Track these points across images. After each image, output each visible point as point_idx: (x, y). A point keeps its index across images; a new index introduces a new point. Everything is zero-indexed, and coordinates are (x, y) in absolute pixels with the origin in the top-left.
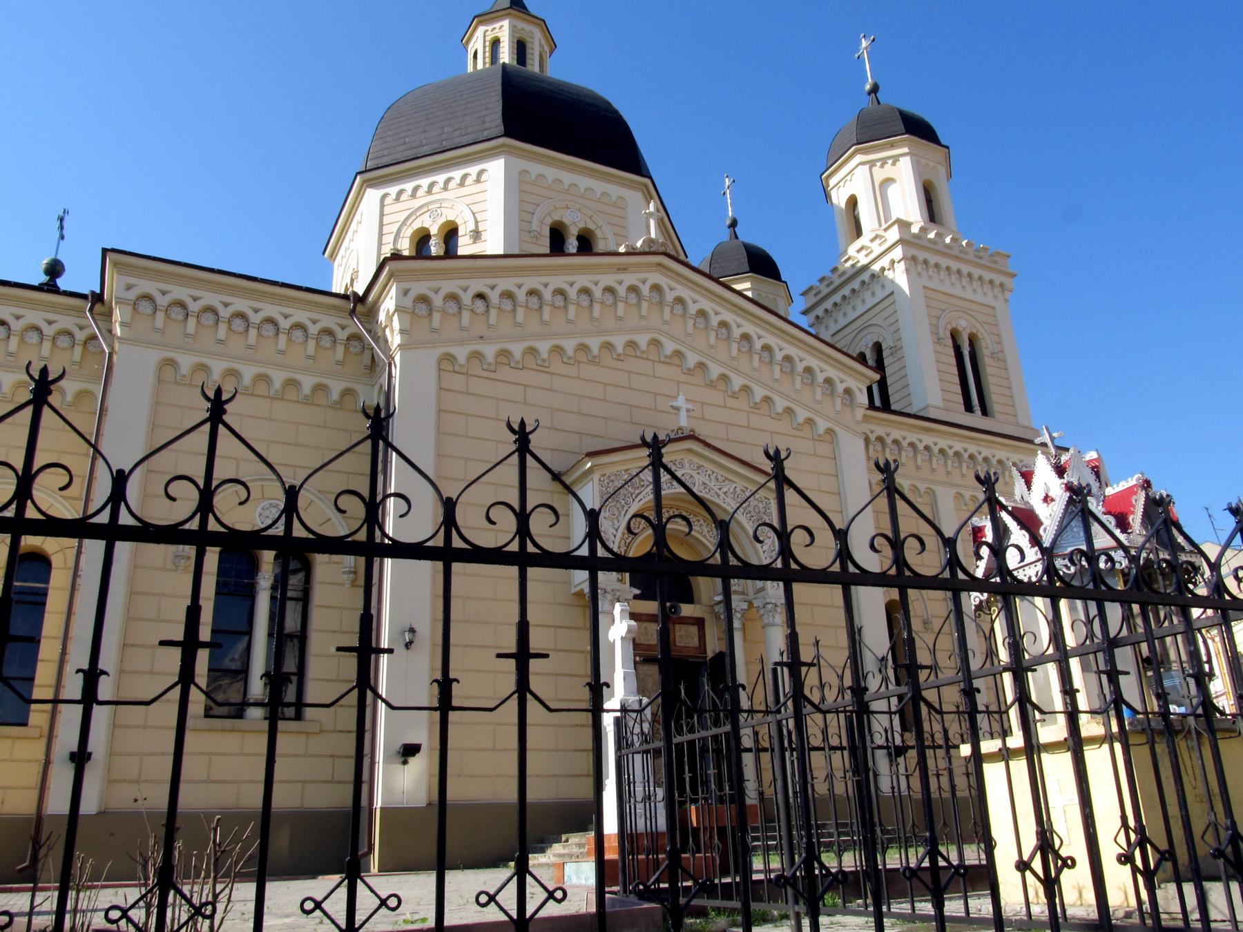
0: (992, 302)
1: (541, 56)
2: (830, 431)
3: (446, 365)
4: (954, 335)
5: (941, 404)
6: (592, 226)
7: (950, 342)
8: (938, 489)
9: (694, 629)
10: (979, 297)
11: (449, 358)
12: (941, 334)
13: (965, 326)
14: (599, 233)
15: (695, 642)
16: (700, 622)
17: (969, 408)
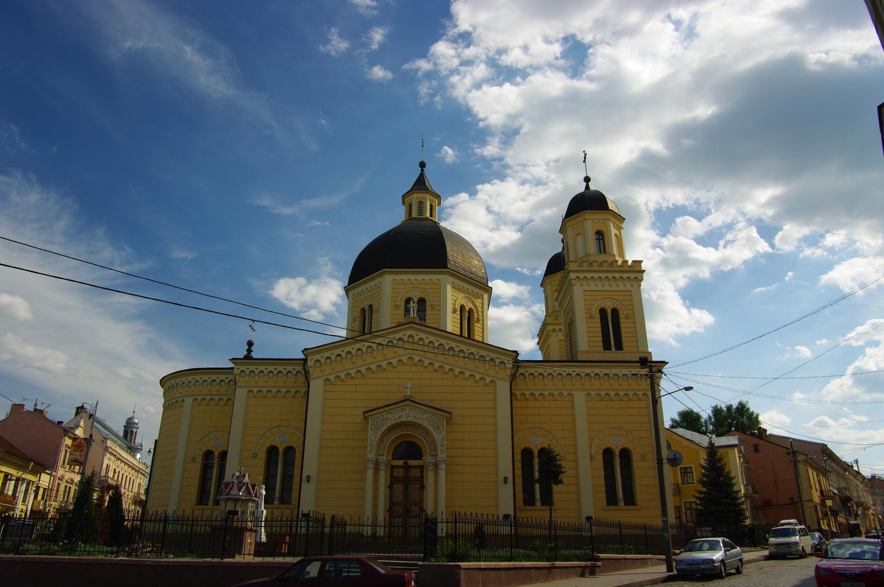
0: (628, 287)
1: (431, 206)
2: (492, 381)
3: (327, 382)
4: (603, 312)
5: (587, 349)
6: (423, 296)
7: (598, 316)
8: (575, 393)
9: (419, 470)
10: (621, 287)
11: (327, 379)
12: (593, 313)
13: (609, 306)
14: (427, 299)
15: (419, 475)
16: (421, 468)
17: (607, 346)
